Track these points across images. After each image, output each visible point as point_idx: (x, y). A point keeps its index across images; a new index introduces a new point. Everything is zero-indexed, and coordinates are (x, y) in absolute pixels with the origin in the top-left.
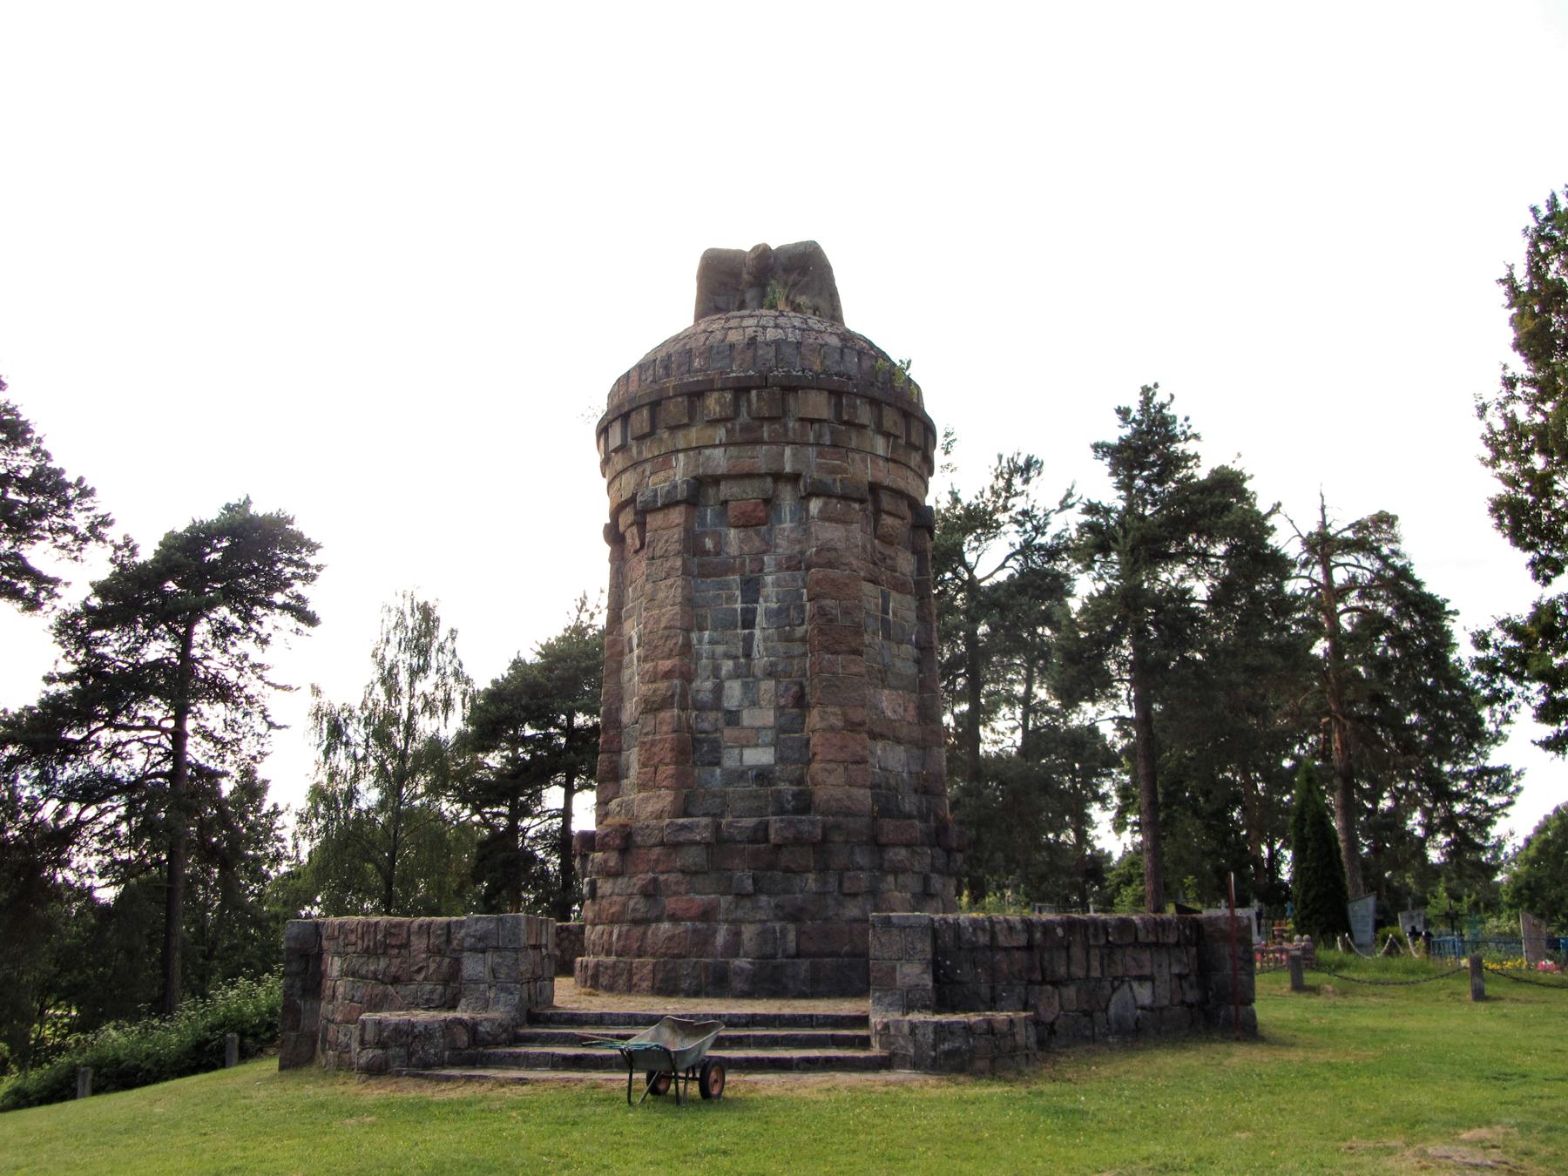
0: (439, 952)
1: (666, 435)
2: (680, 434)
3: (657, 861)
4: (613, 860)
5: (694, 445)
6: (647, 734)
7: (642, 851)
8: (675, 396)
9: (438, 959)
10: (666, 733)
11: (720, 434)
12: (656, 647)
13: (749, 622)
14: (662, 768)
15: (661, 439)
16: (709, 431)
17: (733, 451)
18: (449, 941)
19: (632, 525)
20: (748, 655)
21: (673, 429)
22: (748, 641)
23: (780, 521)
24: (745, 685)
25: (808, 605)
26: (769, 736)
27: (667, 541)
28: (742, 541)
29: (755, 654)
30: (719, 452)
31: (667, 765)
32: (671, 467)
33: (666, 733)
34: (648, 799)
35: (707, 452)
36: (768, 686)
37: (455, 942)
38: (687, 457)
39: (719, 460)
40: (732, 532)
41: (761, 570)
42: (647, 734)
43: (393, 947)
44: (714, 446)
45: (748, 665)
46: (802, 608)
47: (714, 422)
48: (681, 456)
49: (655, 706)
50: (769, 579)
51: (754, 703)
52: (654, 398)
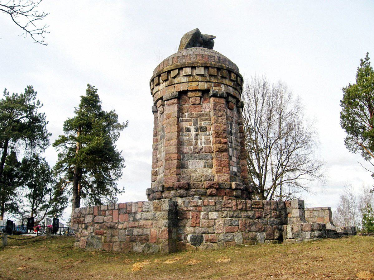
0: (275, 209)
1: (220, 78)
2: (224, 80)
3: (228, 193)
4: (214, 191)
5: (227, 84)
6: (219, 158)
7: (223, 190)
8: (225, 70)
9: (275, 212)
10: (226, 159)
11: (232, 84)
12: (220, 134)
13: (232, 135)
14: (224, 168)
15: (218, 78)
16: (230, 82)
17: (233, 90)
18: (278, 207)
19: (198, 97)
20: (232, 143)
21: (223, 77)
22: (231, 138)
23: (234, 111)
24: (232, 150)
25: (239, 134)
26: (235, 164)
27: (220, 106)
28: (230, 113)
29: (233, 143)
30: (231, 88)
31: (226, 167)
32: (220, 87)
33: (226, 159)
34: (222, 176)
35: (229, 87)
36: (235, 151)
37: (279, 207)
38: (224, 86)
39: (231, 90)
40: (228, 110)
41: (233, 122)
42: (219, 158)
43: (255, 208)
44: (231, 86)
45: (232, 145)
46: (238, 134)
47: (232, 81)
48: (223, 85)
49: (222, 151)
50: (234, 124)
51: (234, 156)
52: (220, 67)
